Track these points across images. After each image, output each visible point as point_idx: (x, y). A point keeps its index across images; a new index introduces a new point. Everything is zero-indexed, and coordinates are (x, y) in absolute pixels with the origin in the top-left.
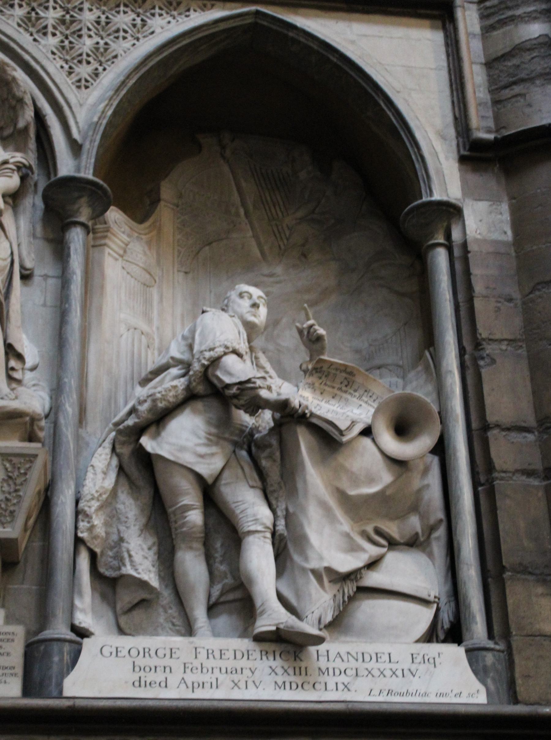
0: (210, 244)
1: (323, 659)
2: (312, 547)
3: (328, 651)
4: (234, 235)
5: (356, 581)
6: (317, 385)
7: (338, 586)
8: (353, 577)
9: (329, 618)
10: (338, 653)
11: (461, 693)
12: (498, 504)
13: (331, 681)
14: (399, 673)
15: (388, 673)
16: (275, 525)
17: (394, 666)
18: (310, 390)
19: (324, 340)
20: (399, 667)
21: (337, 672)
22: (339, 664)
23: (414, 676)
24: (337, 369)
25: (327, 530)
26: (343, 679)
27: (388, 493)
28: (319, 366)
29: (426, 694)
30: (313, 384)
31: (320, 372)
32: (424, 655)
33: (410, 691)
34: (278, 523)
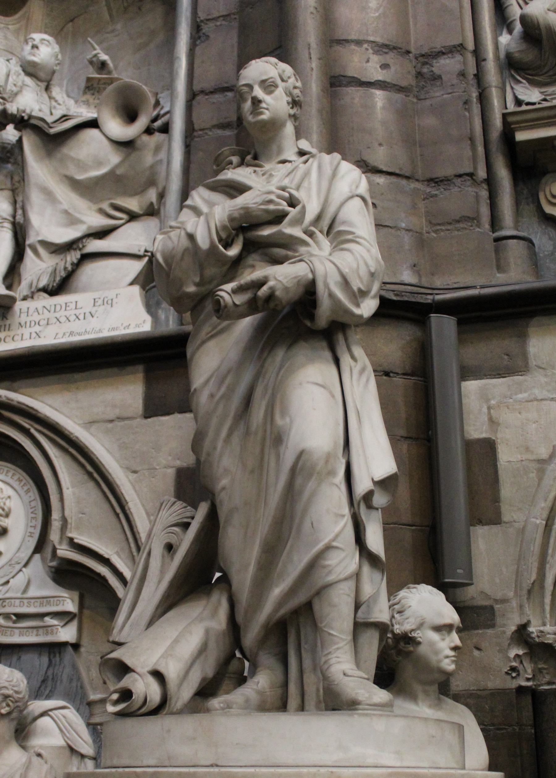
0: (72, 21)
1: (23, 316)
2: (33, 227)
3: (28, 308)
4: (91, 9)
5: (80, 249)
6: (91, 101)
7: (62, 256)
8: (75, 246)
9: (43, 282)
10: (36, 309)
11: (130, 325)
12: (192, 158)
13: (26, 332)
14: (81, 317)
15: (72, 318)
16: (14, 217)
17: (77, 312)
18: (84, 106)
19: (108, 64)
20: (82, 311)
21: (33, 323)
22: (36, 317)
23: (93, 317)
24: (105, 84)
25: (49, 211)
26: (37, 328)
27: (118, 172)
28: (90, 84)
29: (100, 331)
30: (88, 101)
31: (92, 89)
32: (104, 299)
33: (88, 330)
34: (17, 213)
